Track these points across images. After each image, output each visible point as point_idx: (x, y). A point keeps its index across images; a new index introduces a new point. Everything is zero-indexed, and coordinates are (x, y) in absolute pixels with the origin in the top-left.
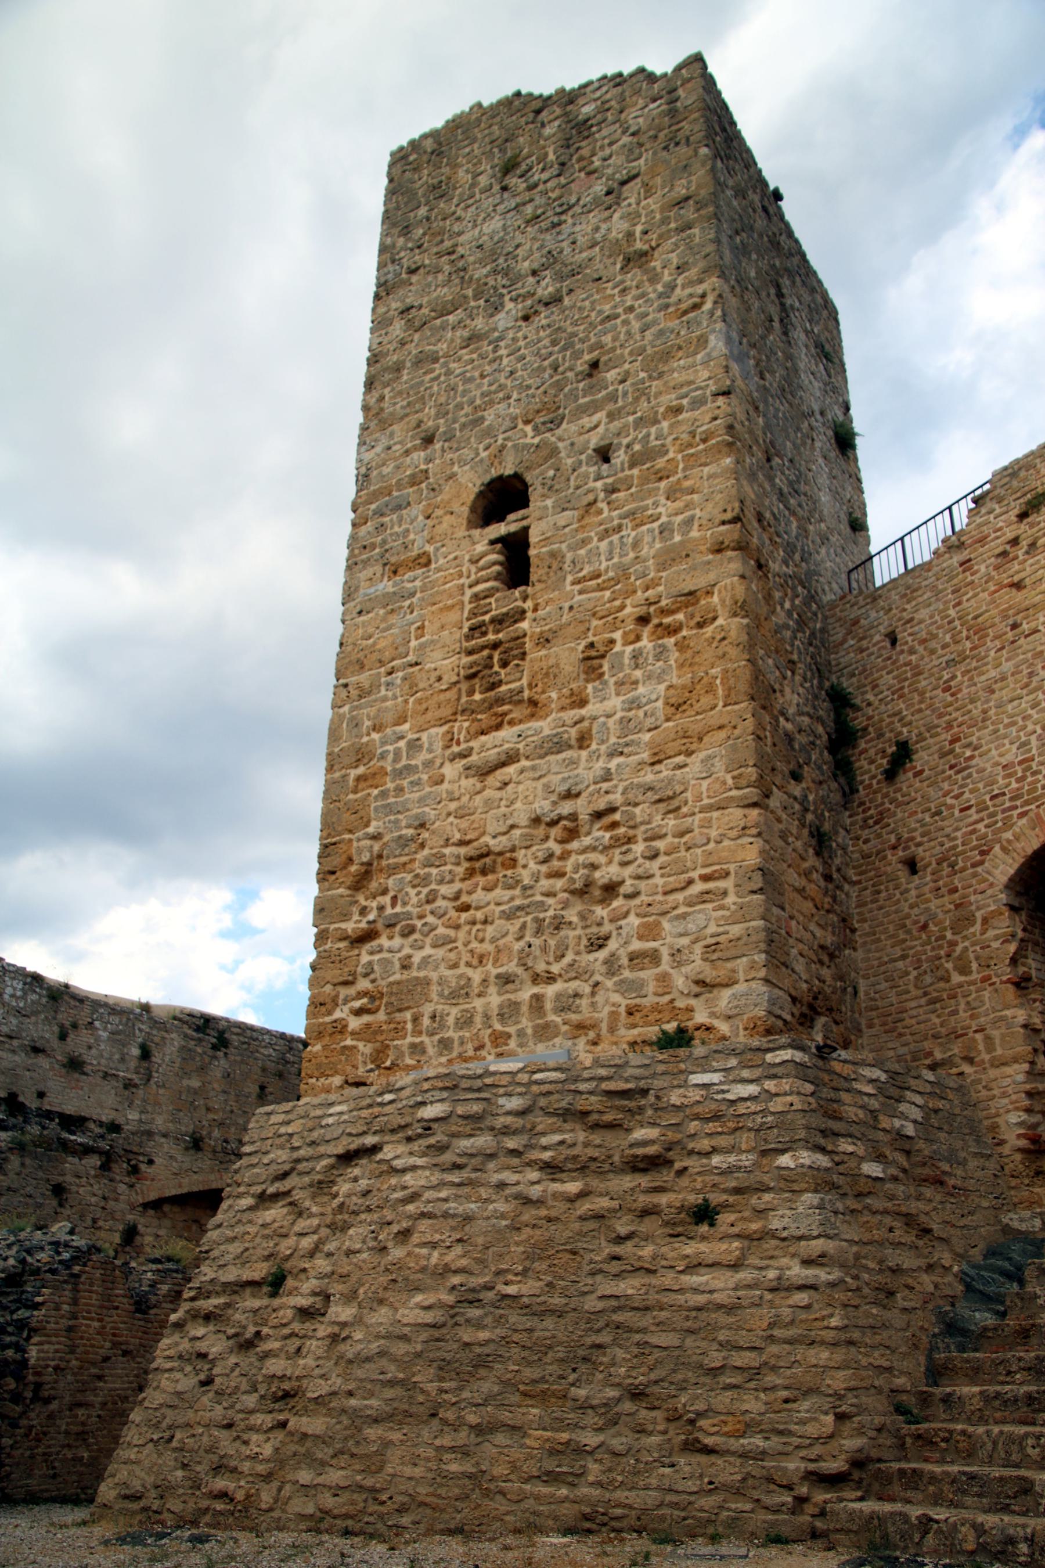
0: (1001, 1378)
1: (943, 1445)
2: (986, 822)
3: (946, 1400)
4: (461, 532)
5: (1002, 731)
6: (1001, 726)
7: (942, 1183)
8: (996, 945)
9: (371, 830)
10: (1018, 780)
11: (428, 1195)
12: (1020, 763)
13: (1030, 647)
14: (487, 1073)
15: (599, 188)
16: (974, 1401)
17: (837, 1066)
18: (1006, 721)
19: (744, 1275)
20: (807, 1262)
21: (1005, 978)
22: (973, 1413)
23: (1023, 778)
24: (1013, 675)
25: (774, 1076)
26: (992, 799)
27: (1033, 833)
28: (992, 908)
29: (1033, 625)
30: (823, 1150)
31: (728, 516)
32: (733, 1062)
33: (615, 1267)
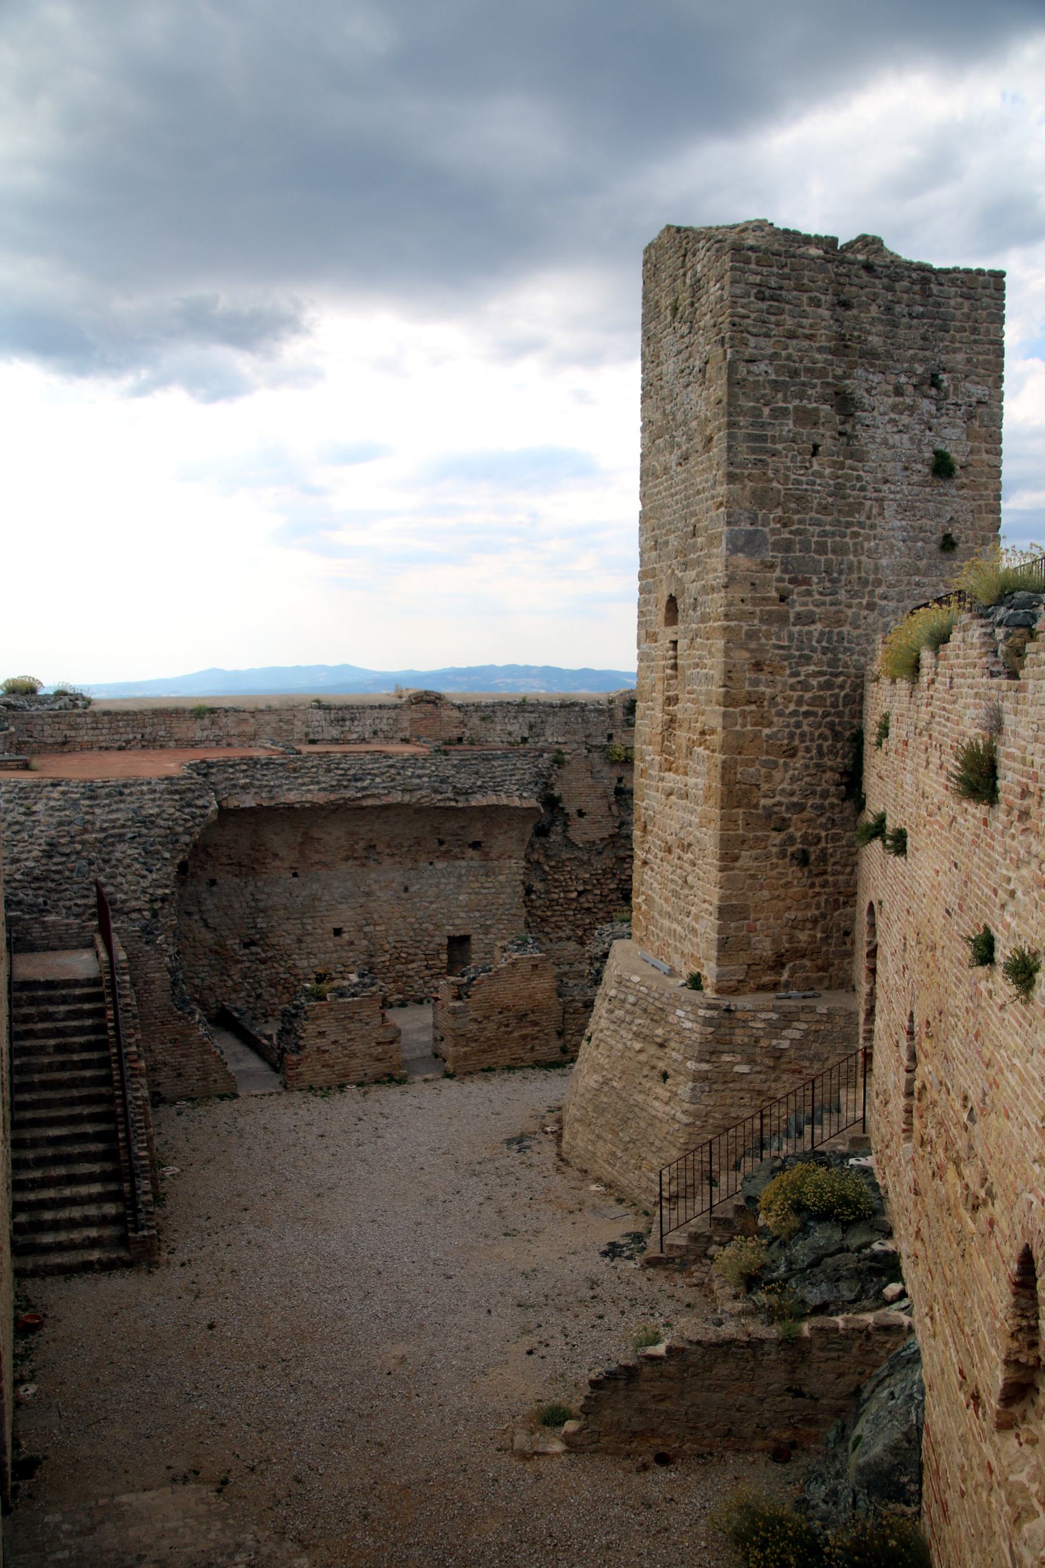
4: (663, 628)
7: (800, 1072)
9: (644, 804)
11: (605, 1032)
14: (629, 980)
15: (698, 364)
17: (739, 1015)
19: (667, 1109)
20: (683, 1112)
25: (697, 1022)
30: (708, 1062)
31: (721, 684)
32: (689, 1009)
33: (639, 1088)
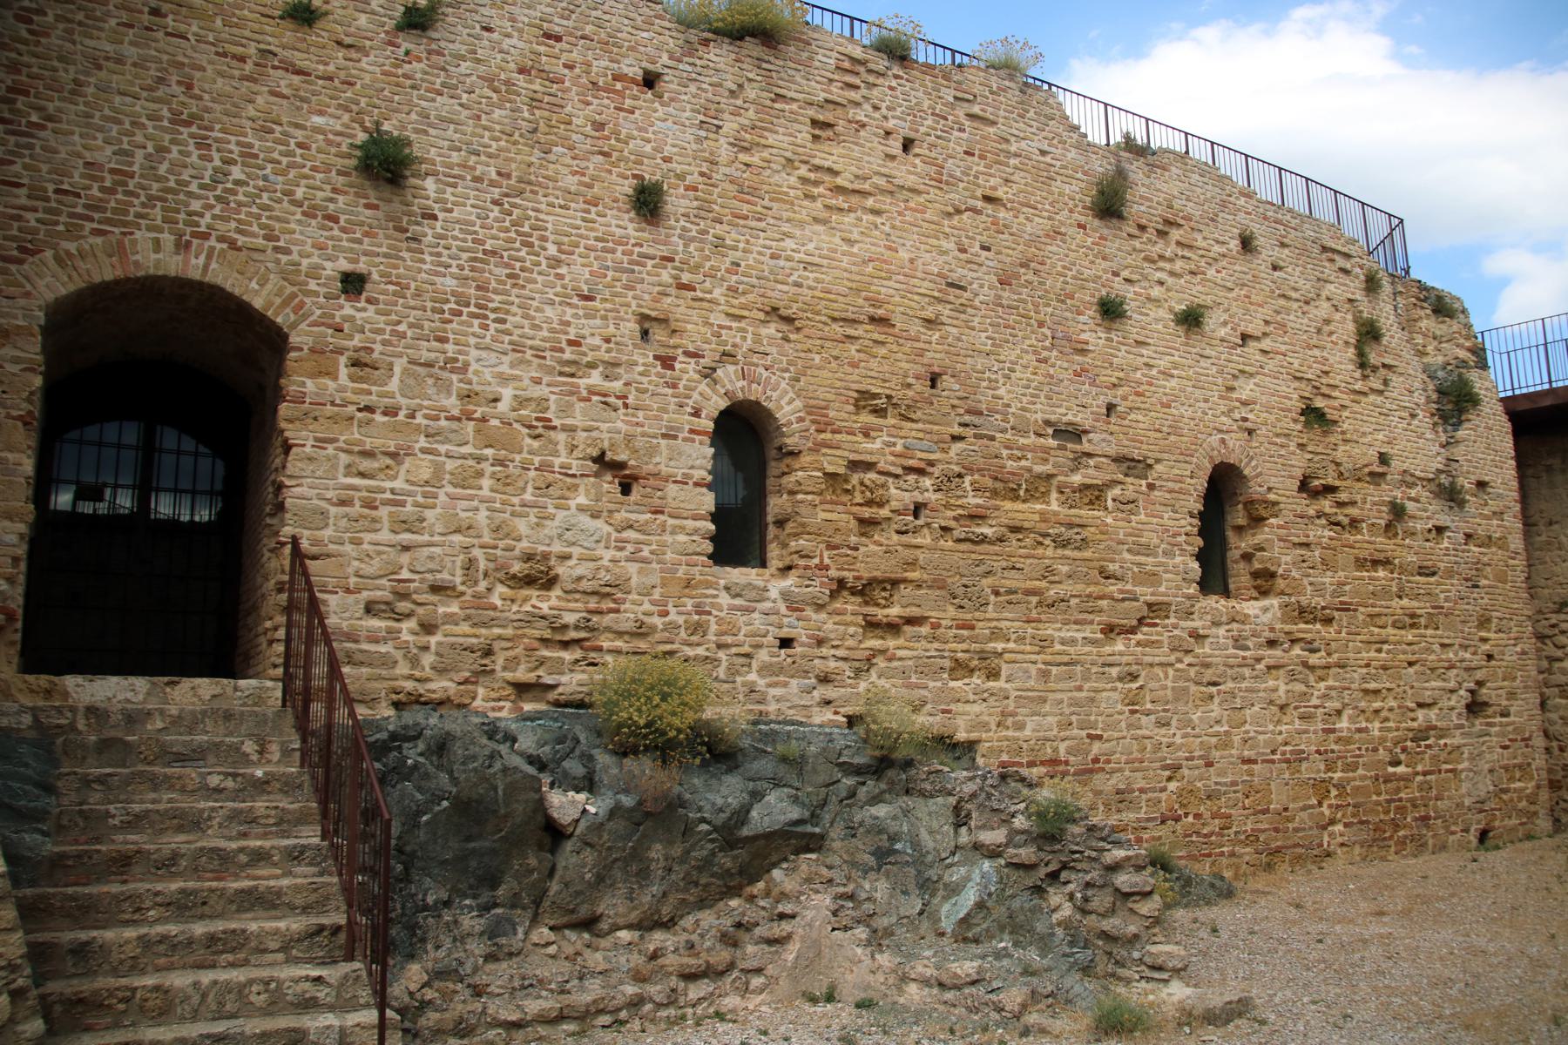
0: (127, 917)
1: (122, 1006)
2: (40, 215)
3: (81, 951)
5: (96, 121)
6: (98, 114)
8: (12, 368)
10: (102, 189)
12: (113, 171)
13: (170, 49)
16: (127, 948)
18: (107, 112)
21: (15, 413)
22: (121, 962)
23: (112, 191)
24: (135, 65)
26: (57, 191)
27: (107, 260)
28: (21, 323)
29: (183, 27)
